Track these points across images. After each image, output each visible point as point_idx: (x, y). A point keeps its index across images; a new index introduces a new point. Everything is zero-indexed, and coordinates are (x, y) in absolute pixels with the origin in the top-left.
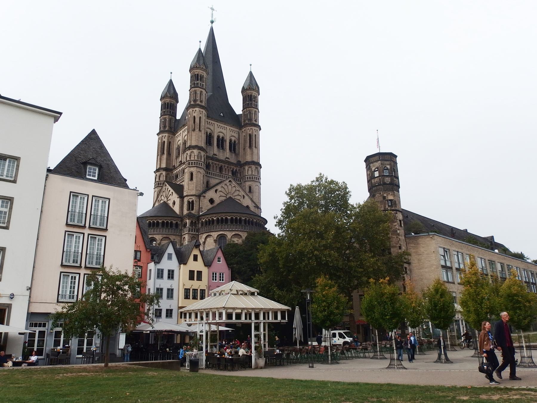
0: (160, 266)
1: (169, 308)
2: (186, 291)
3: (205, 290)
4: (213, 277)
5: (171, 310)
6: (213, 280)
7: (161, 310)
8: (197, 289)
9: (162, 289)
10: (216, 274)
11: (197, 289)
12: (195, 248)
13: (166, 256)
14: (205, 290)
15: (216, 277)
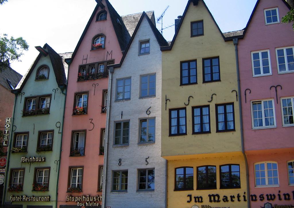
0: (119, 74)
1: (144, 166)
2: (174, 114)
3: (232, 104)
4: (257, 64)
5: (151, 171)
6: (258, 71)
7: (126, 173)
8: (208, 106)
9: (127, 124)
10: (265, 55)
11: (208, 106)
12: (192, 5)
13: (135, 47)
14: (232, 104)
15: (265, 63)
